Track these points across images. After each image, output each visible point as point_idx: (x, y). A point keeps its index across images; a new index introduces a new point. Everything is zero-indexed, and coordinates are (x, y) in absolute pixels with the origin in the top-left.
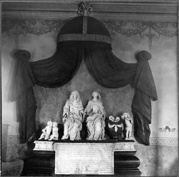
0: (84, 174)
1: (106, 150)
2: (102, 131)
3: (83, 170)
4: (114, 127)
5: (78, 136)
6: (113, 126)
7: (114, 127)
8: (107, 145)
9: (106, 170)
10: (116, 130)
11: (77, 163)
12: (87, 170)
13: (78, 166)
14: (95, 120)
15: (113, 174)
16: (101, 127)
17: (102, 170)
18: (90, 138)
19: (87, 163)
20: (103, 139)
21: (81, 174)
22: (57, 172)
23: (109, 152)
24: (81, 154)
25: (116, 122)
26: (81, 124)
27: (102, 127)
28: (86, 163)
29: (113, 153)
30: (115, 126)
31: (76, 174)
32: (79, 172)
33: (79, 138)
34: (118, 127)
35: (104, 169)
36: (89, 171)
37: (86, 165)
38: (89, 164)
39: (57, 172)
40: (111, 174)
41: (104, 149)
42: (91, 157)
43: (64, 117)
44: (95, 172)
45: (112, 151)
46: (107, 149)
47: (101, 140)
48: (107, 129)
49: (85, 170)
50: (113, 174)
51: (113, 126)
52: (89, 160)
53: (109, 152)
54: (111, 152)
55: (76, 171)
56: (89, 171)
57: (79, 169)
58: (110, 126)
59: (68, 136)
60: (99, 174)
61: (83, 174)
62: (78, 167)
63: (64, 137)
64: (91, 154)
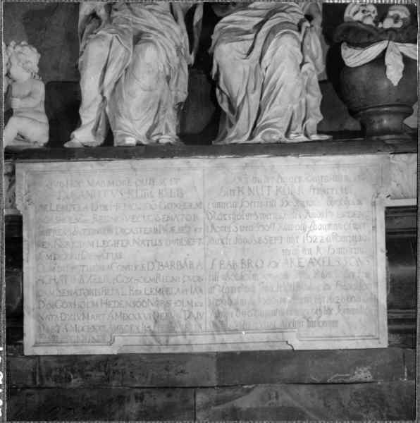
0: (203, 349)
1: (336, 197)
2: (307, 90)
3: (194, 328)
4: (380, 61)
5: (161, 128)
6: (373, 51)
7: (380, 61)
8: (338, 165)
9: (335, 323)
10: (394, 73)
11: (160, 285)
12: (220, 326)
13: (167, 304)
14: (259, 27)
15: (385, 345)
16: (301, 65)
17: (310, 324)
18: (239, 132)
19: (221, 282)
20: (315, 137)
21: (186, 350)
22: (37, 344)
23: (352, 208)
24: (181, 230)
25: (391, 29)
26: (180, 65)
27: (305, 68)
28: (215, 279)
29: (381, 216)
30: (384, 51)
31: (155, 350)
32: (172, 340)
33: (168, 135)
34: (406, 60)
35: (324, 318)
36: (236, 331)
37: (217, 294)
38: (233, 290)
39: (37, 344)
40: (371, 344)
41: (324, 191)
42: (245, 241)
43: (82, 36)
44: (272, 336)
45: (374, 204)
46: (345, 190)
47: (302, 138)
48: (335, 77)
49: (209, 327)
50: (385, 345)
51: (373, 51)
52: (234, 266)
53: (352, 208)
54: (365, 207)
55: (153, 334)
56: (236, 331)
57: (169, 315)
58: (354, 58)
59: (102, 130)
60: (298, 345)
61: (196, 350)
62: (161, 311)
63: (83, 136)
64: (244, 228)
